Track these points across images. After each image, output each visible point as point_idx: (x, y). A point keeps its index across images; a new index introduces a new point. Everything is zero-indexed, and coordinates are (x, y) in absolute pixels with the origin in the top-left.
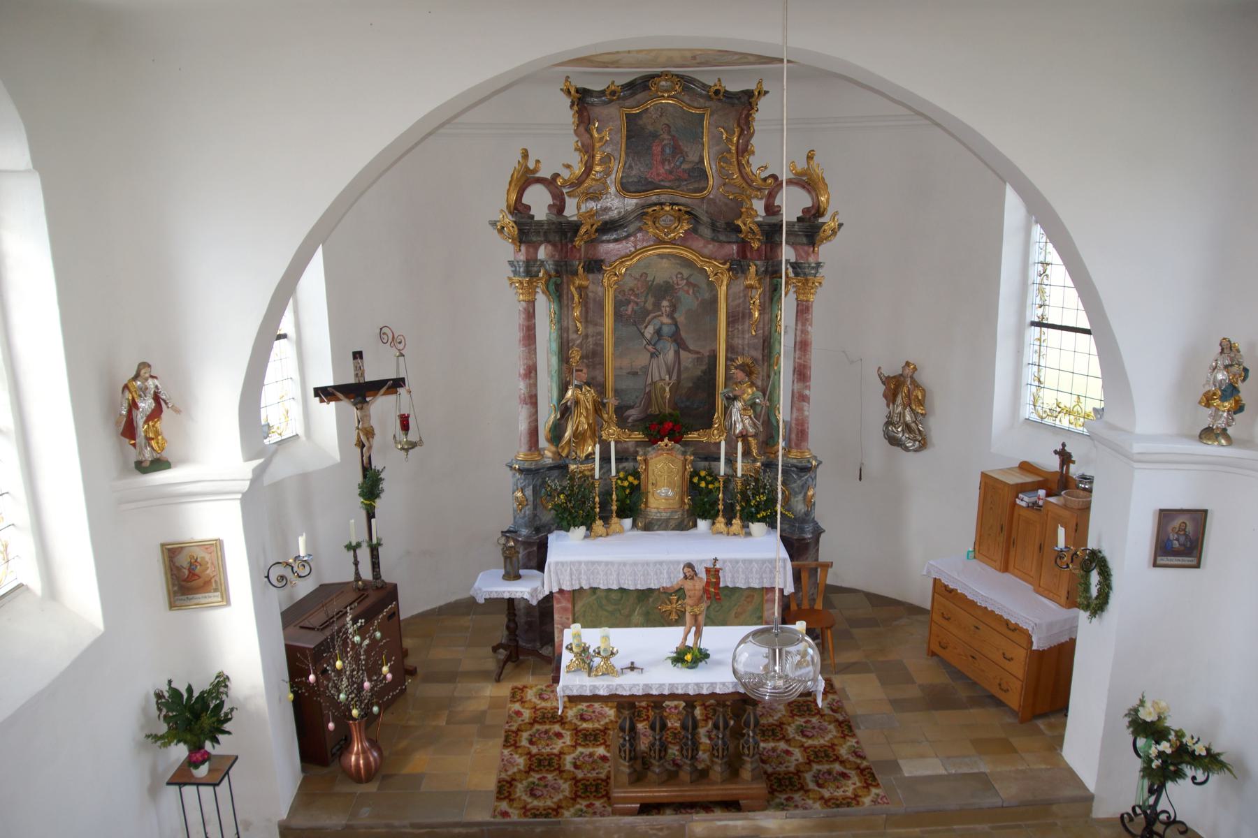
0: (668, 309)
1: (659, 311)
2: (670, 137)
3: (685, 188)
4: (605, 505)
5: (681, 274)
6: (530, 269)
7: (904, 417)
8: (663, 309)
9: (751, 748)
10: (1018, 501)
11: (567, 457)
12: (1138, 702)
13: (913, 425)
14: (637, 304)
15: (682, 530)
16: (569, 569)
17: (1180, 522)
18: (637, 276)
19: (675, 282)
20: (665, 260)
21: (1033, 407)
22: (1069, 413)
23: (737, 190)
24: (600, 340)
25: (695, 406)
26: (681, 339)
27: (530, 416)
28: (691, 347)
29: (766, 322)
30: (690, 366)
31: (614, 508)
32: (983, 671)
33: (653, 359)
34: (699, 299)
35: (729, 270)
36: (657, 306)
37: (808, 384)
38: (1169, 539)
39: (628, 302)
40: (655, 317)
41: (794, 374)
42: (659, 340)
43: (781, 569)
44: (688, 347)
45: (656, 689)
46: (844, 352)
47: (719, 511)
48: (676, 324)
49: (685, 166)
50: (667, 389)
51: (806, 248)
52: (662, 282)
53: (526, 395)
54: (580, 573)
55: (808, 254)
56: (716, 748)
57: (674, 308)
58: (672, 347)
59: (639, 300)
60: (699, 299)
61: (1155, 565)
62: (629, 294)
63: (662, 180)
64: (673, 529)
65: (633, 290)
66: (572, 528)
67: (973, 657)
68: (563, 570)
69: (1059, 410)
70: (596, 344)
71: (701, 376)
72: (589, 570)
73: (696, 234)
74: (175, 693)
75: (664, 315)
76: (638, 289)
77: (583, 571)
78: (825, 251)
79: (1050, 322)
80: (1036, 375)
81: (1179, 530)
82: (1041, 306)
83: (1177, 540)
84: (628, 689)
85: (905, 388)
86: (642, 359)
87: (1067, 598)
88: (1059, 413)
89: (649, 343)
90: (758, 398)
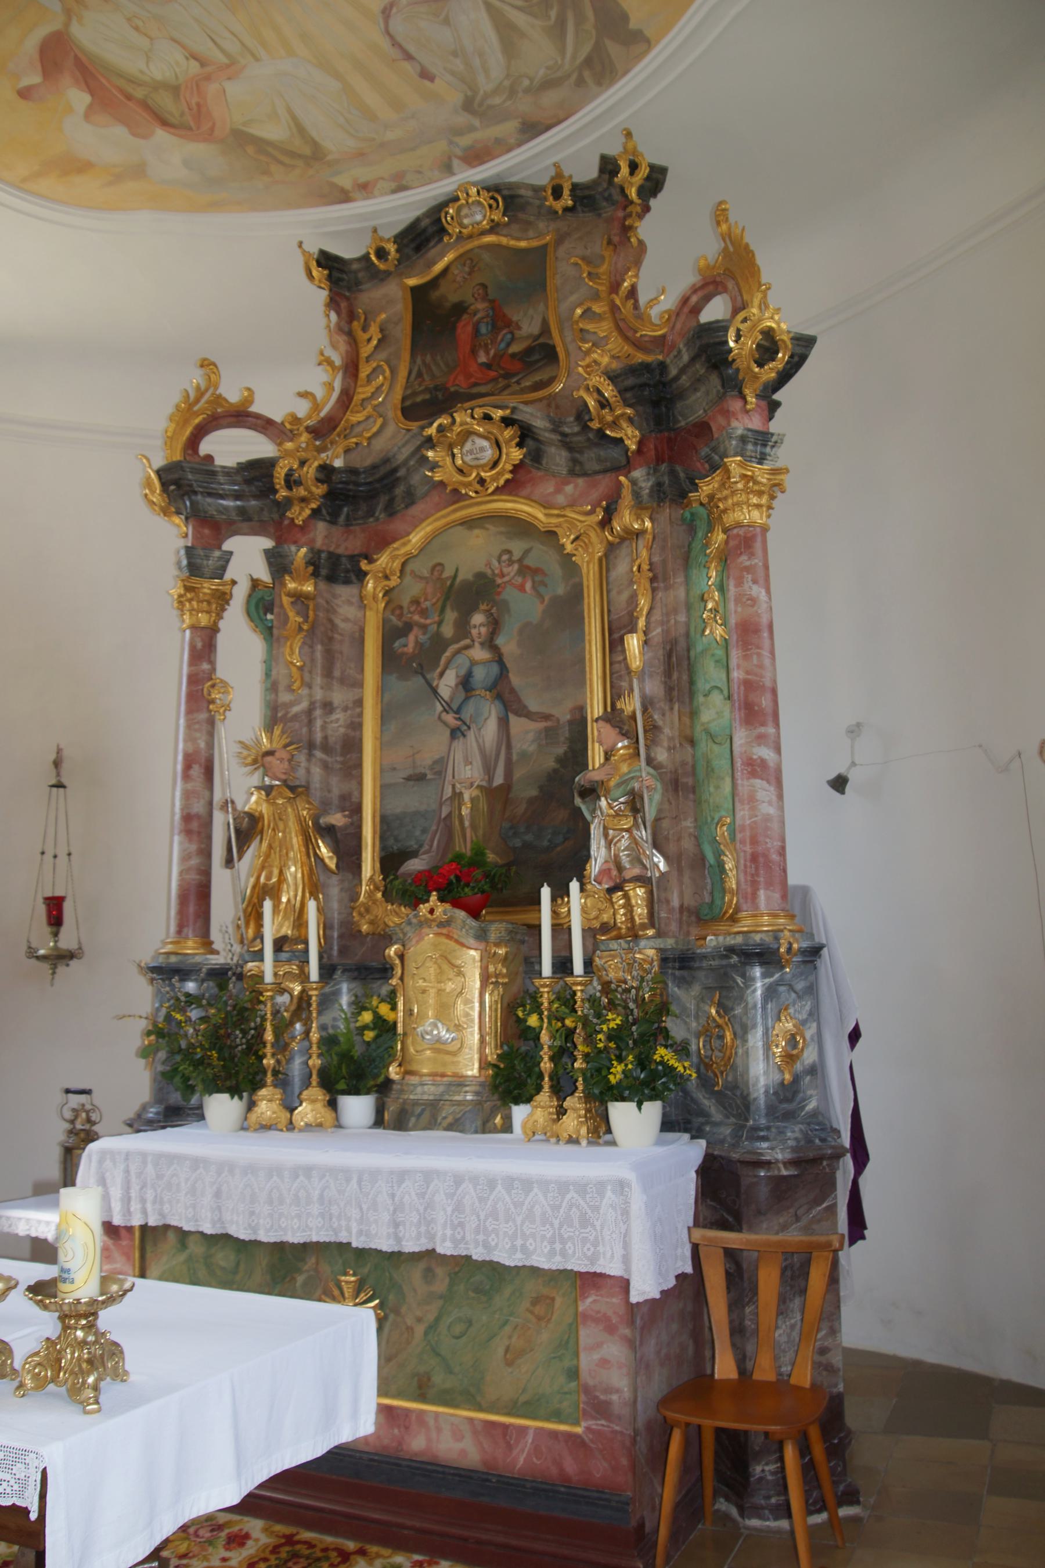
0: (483, 630)
3: (517, 388)
5: (509, 552)
8: (474, 632)
14: (424, 627)
18: (426, 573)
19: (497, 572)
20: (476, 532)
25: (546, 843)
26: (512, 691)
28: (533, 706)
30: (532, 748)
33: (455, 743)
34: (547, 599)
36: (463, 628)
40: (458, 652)
42: (467, 698)
44: (525, 707)
46: (980, 746)
48: (499, 660)
49: (515, 348)
52: (470, 577)
57: (495, 625)
59: (428, 621)
60: (547, 599)
63: (476, 385)
71: (555, 771)
72: (160, 1177)
73: (538, 469)
75: (477, 644)
76: (426, 600)
89: (447, 708)
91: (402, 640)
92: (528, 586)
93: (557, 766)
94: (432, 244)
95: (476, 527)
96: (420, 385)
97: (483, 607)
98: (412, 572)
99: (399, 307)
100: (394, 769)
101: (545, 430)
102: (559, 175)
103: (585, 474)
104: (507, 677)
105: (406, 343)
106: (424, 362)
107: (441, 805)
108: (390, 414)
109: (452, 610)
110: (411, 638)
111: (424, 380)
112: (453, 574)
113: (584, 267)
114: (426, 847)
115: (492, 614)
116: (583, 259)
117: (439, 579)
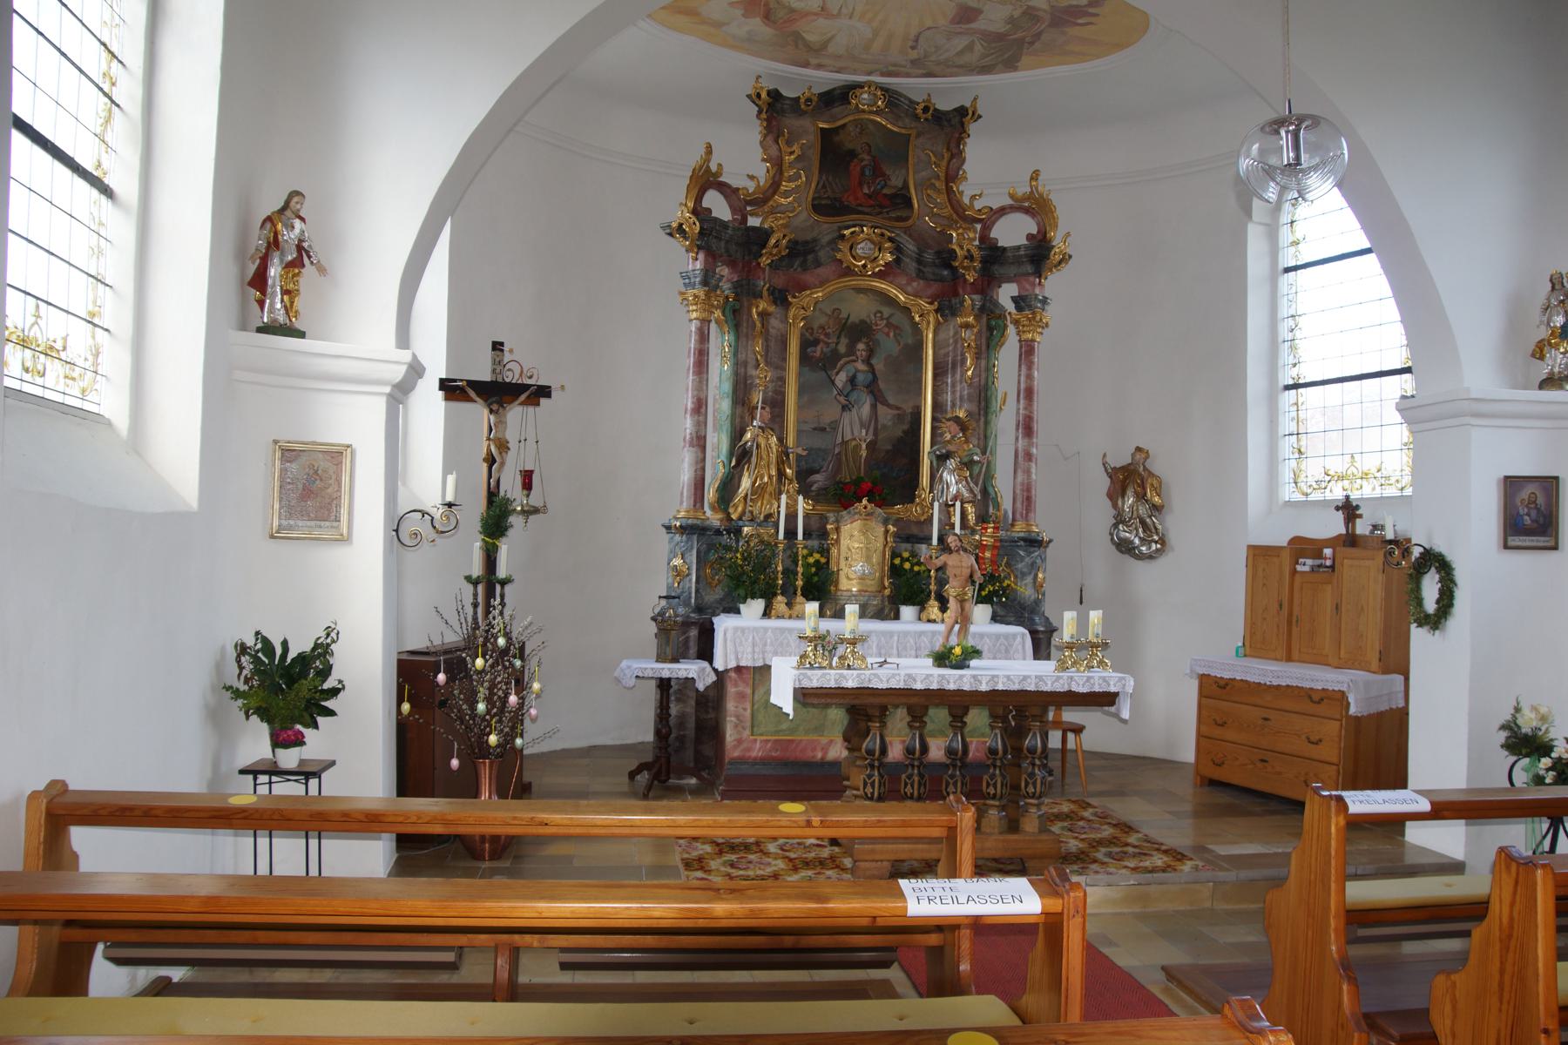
2: (869, 158)
4: (789, 573)
5: (881, 312)
6: (708, 279)
7: (1137, 510)
8: (858, 353)
9: (1039, 782)
10: (1299, 568)
11: (740, 518)
12: (1512, 711)
13: (1148, 520)
14: (827, 344)
15: (882, 620)
16: (751, 638)
17: (1528, 493)
18: (829, 313)
20: (862, 295)
21: (1294, 485)
22: (1341, 478)
23: (946, 222)
24: (780, 386)
26: (880, 391)
27: (697, 463)
28: (891, 401)
29: (983, 369)
31: (800, 583)
32: (1280, 773)
33: (845, 414)
35: (937, 311)
36: (851, 350)
37: (1035, 440)
38: (1518, 513)
39: (816, 342)
40: (848, 362)
41: (1017, 429)
42: (852, 390)
43: (1020, 647)
44: (887, 401)
45: (922, 682)
47: (930, 592)
48: (873, 372)
49: (885, 191)
50: (864, 446)
51: (1031, 279)
52: (857, 321)
53: (694, 435)
54: (765, 645)
55: (1033, 285)
56: (992, 783)
57: (871, 352)
58: (868, 400)
59: (830, 341)
61: (1506, 547)
62: (817, 333)
63: (861, 205)
64: (872, 617)
65: (824, 329)
66: (749, 600)
67: (1262, 761)
68: (743, 639)
69: (1328, 478)
70: (775, 392)
72: (777, 640)
74: (268, 646)
76: (829, 328)
77: (769, 641)
78: (1053, 285)
79: (1308, 380)
80: (1295, 446)
81: (1529, 503)
82: (1295, 365)
83: (1528, 514)
84: (885, 679)
85: (1136, 476)
86: (830, 412)
87: (1380, 660)
88: (1329, 481)
89: (840, 393)
90: (977, 454)
91: (813, 349)
92: (892, 334)
93: (902, 435)
94: (836, 104)
95: (862, 293)
96: (824, 193)
97: (864, 340)
98: (820, 309)
99: (812, 137)
101: (914, 252)
102: (929, 101)
105: (816, 164)
106: (827, 180)
108: (804, 206)
109: (845, 336)
110: (819, 348)
111: (827, 191)
112: (846, 316)
113: (933, 159)
114: (825, 469)
116: (932, 152)
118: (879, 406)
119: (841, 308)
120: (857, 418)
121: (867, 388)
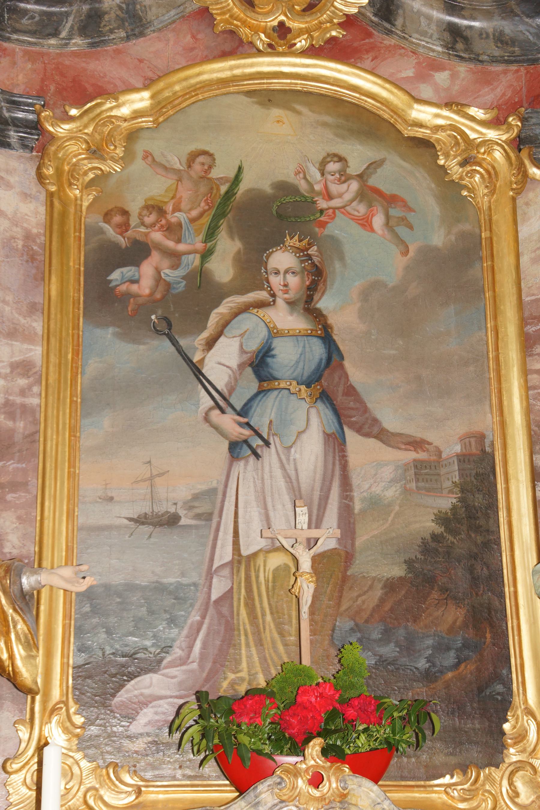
0: (293, 281)
1: (262, 289)
5: (341, 159)
8: (276, 281)
19: (317, 187)
20: (276, 112)
25: (422, 664)
33: (239, 467)
40: (245, 309)
42: (261, 392)
44: (375, 421)
52: (266, 187)
58: (315, 421)
59: (181, 247)
60: (412, 249)
62: (143, 224)
65: (161, 212)
71: (435, 537)
73: (389, 32)
75: (280, 302)
76: (177, 209)
91: (128, 271)
92: (378, 221)
93: (439, 530)
97: (294, 242)
98: (147, 155)
100: (111, 499)
103: (477, 60)
104: (341, 366)
107: (210, 575)
112: (232, 174)
114: (177, 652)
115: (310, 257)
117: (204, 177)
118: (350, 436)
119: (207, 149)
120: (281, 483)
121: (308, 386)
